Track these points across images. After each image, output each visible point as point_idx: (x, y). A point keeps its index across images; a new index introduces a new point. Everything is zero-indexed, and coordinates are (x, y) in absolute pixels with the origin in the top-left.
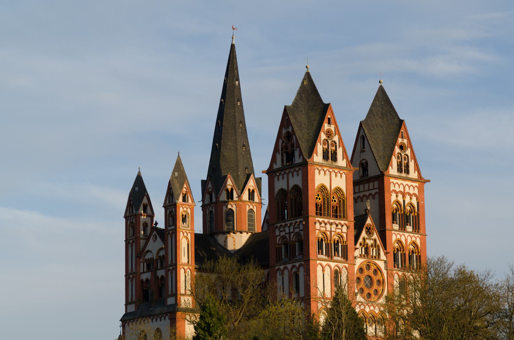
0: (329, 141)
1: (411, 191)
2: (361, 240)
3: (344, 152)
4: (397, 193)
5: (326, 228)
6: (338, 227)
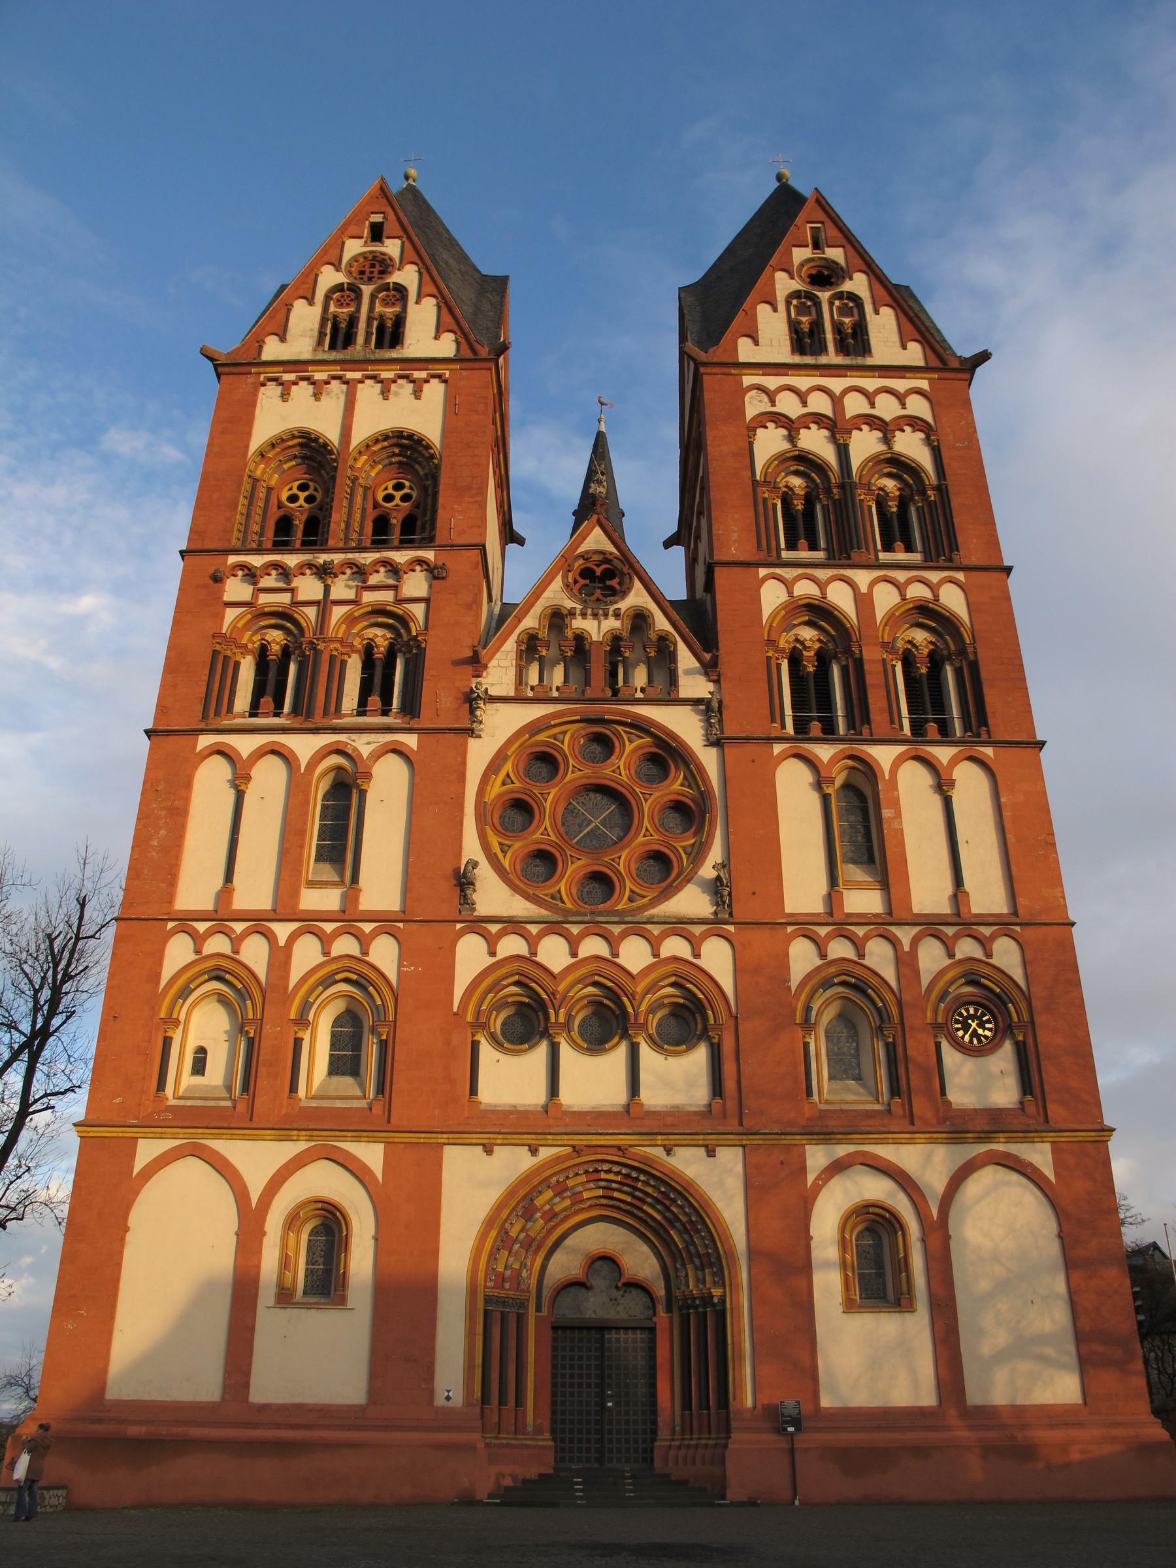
0: (362, 287)
1: (887, 408)
2: (530, 622)
3: (445, 311)
4: (791, 427)
5: (292, 591)
6: (374, 579)
